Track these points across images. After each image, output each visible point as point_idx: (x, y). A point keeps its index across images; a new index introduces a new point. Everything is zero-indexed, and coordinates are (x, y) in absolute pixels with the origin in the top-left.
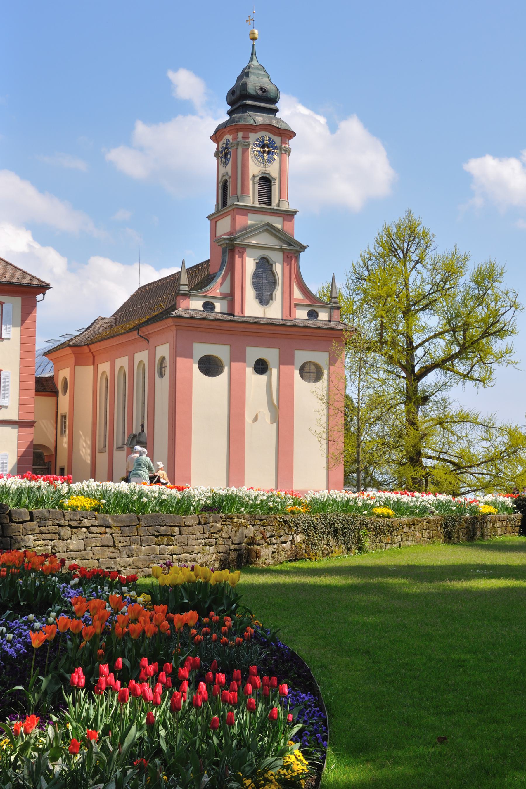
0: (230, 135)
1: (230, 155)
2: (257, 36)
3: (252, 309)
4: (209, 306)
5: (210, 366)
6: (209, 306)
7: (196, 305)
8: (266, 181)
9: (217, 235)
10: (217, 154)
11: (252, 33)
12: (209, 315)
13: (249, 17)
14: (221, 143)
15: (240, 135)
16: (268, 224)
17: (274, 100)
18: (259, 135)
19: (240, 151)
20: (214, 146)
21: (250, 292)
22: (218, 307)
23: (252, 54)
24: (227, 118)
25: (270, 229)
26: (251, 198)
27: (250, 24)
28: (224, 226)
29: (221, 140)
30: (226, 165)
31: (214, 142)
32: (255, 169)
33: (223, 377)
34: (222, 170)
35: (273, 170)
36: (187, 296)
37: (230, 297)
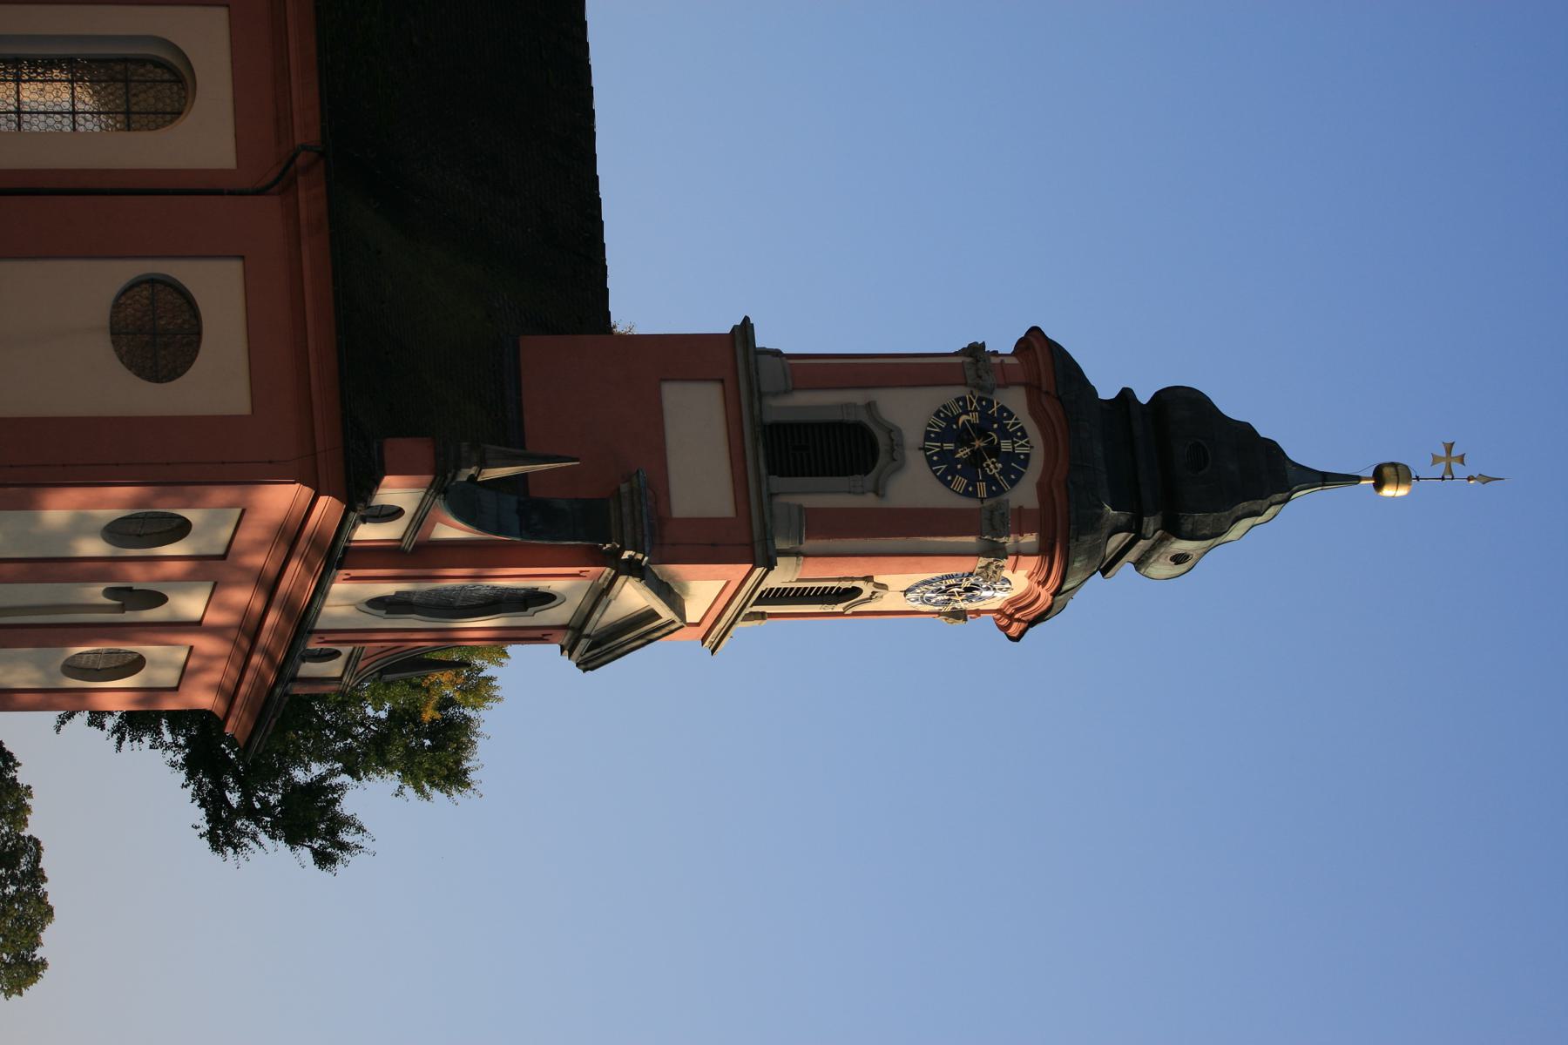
0: (1040, 486)
1: (966, 493)
2: (1388, 491)
10: (975, 351)
11: (1401, 474)
13: (1461, 459)
14: (1015, 400)
24: (1107, 391)
27: (1436, 460)
29: (1033, 413)
31: (1021, 341)
34: (911, 414)
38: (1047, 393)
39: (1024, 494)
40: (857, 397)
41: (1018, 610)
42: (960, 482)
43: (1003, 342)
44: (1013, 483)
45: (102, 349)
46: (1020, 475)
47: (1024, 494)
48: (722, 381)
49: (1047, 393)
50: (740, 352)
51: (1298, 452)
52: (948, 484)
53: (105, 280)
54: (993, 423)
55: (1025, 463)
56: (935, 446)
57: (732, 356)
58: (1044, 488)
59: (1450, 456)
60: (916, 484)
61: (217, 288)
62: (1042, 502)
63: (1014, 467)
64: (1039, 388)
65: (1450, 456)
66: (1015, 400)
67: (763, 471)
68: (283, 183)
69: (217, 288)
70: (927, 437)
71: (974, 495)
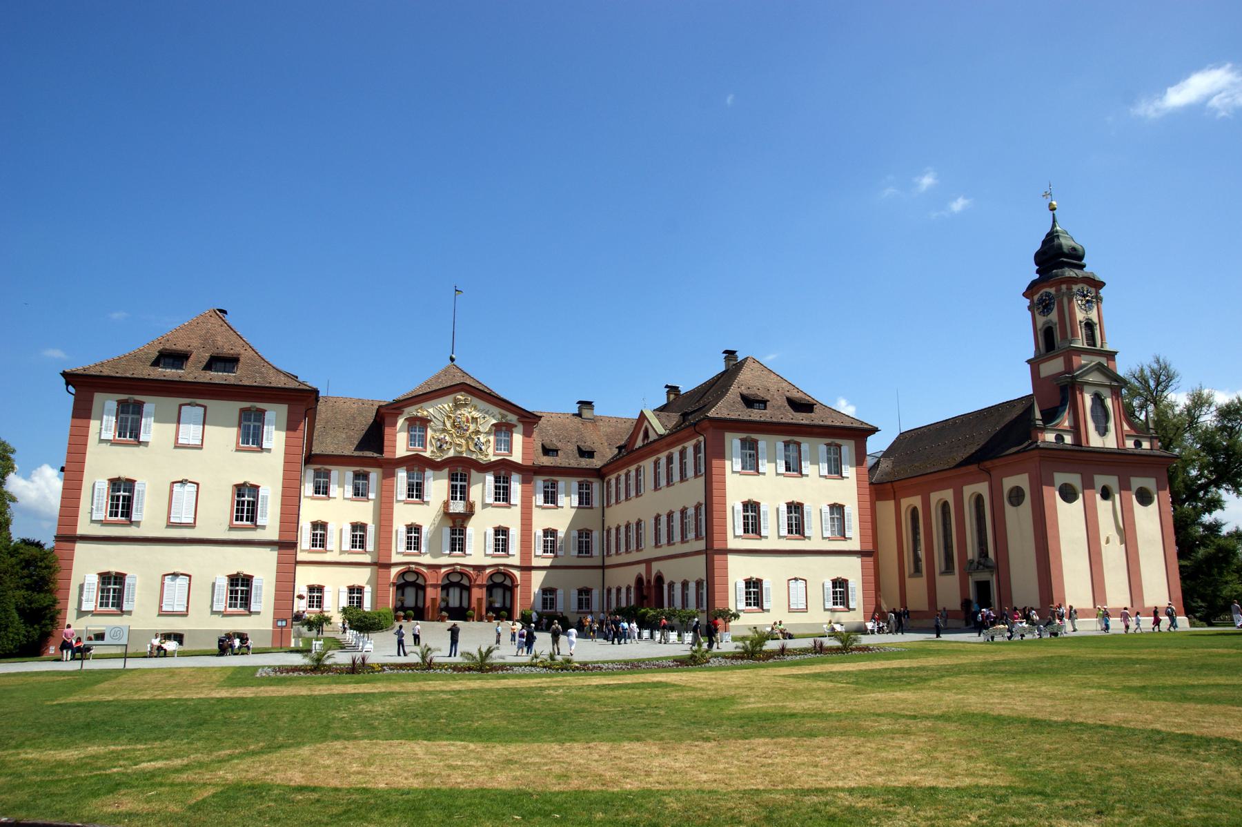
3: (1095, 441)
4: (1060, 438)
5: (1068, 495)
6: (1060, 438)
7: (1050, 437)
8: (1089, 325)
9: (1042, 375)
10: (1029, 308)
11: (1050, 204)
12: (1060, 445)
14: (1036, 297)
15: (1064, 287)
16: (1100, 364)
17: (1081, 258)
18: (1079, 286)
19: (1065, 300)
20: (1027, 302)
21: (1091, 425)
22: (1068, 439)
23: (1054, 221)
24: (1037, 276)
25: (1100, 368)
26: (1081, 342)
28: (1054, 366)
32: (1080, 316)
33: (1079, 503)
34: (1041, 320)
35: (1093, 315)
36: (1043, 430)
37: (1076, 430)
39: (1052, 291)
43: (1027, 302)
45: (1021, 508)
47: (1052, 291)
51: (1048, 230)
53: (1008, 507)
54: (1041, 301)
57: (1034, 364)
58: (1051, 287)
59: (1045, 195)
60: (1054, 316)
61: (1009, 483)
63: (1048, 294)
65: (1045, 195)
66: (1036, 297)
68: (988, 471)
69: (1009, 483)
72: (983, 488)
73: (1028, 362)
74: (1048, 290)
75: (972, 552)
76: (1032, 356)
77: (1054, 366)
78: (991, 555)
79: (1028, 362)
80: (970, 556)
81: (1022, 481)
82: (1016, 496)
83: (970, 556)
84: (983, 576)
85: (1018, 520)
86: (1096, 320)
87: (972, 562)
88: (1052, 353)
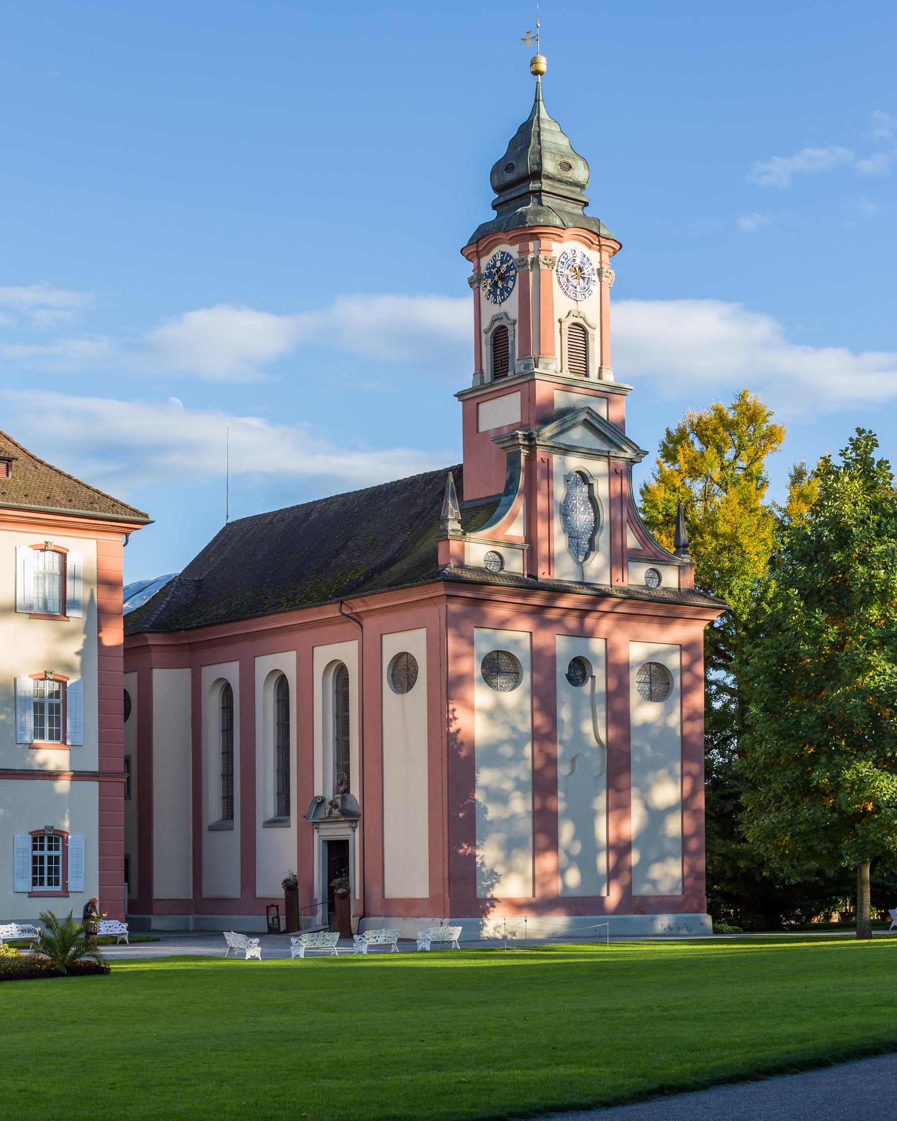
0: (512, 245)
1: (514, 281)
2: (543, 67)
14: (485, 261)
20: (468, 268)
24: (492, 215)
28: (501, 413)
29: (488, 253)
30: (503, 300)
34: (490, 310)
38: (477, 248)
39: (514, 251)
40: (484, 336)
41: (593, 243)
42: (510, 284)
44: (511, 257)
46: (508, 255)
48: (478, 404)
49: (477, 248)
50: (466, 397)
52: (511, 290)
55: (503, 253)
56: (499, 298)
57: (470, 400)
60: (511, 306)
62: (516, 243)
64: (477, 252)
67: (507, 379)
70: (495, 302)
71: (514, 276)
72: (347, 652)
73: (460, 395)
74: (505, 248)
75: (323, 785)
76: (467, 382)
77: (501, 413)
78: (355, 790)
79: (460, 395)
80: (318, 792)
81: (413, 642)
82: (403, 673)
83: (318, 792)
84: (339, 831)
85: (404, 719)
86: (593, 319)
87: (323, 800)
88: (502, 383)
